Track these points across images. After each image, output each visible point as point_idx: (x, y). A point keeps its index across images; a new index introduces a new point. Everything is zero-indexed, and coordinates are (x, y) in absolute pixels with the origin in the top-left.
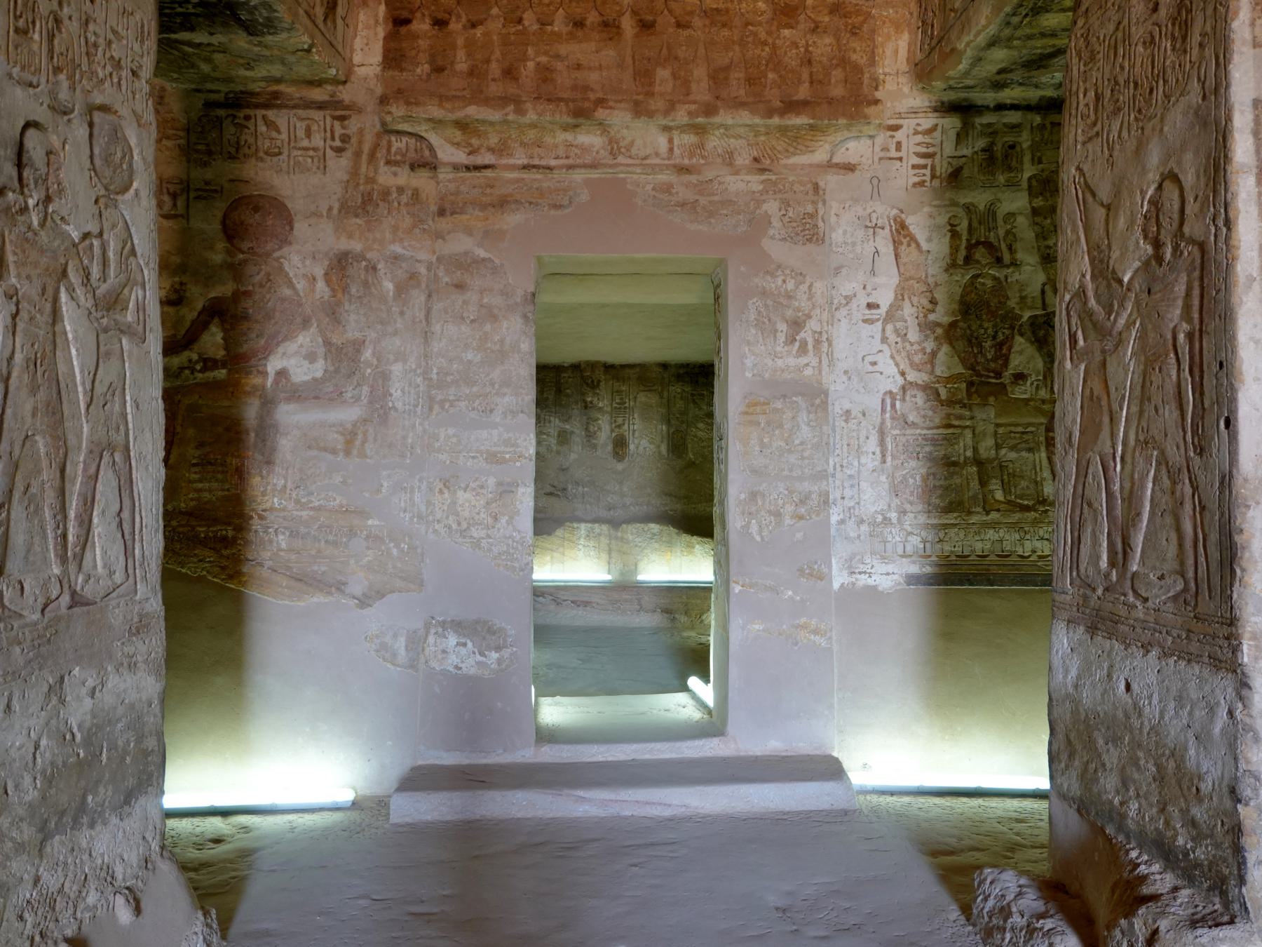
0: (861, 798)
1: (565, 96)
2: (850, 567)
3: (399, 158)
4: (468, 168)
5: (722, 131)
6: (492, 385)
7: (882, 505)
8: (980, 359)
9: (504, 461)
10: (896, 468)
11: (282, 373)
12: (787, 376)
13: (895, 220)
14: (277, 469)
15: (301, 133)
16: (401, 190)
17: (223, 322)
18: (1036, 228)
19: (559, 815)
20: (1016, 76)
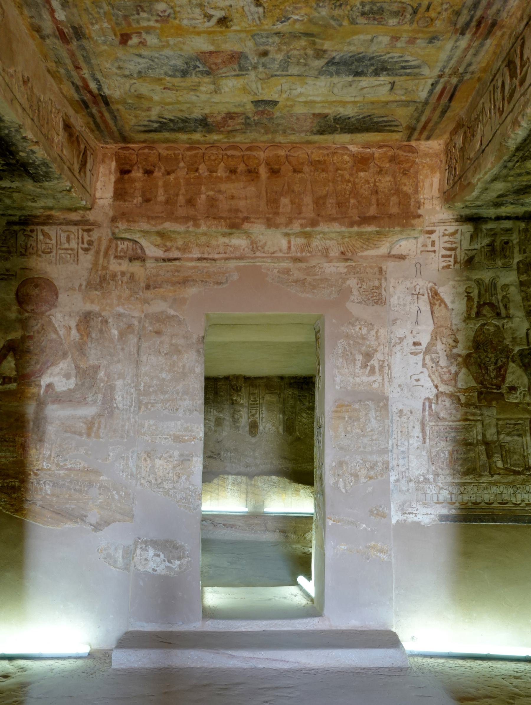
0: (411, 659)
1: (224, 216)
2: (402, 510)
3: (122, 254)
4: (164, 260)
5: (321, 235)
6: (178, 393)
7: (423, 470)
8: (486, 377)
9: (183, 441)
10: (432, 446)
11: (50, 386)
12: (362, 388)
13: (431, 290)
14: (46, 445)
15: (64, 240)
16: (123, 274)
17: (15, 354)
18: (523, 294)
19: (217, 666)
20: (509, 199)
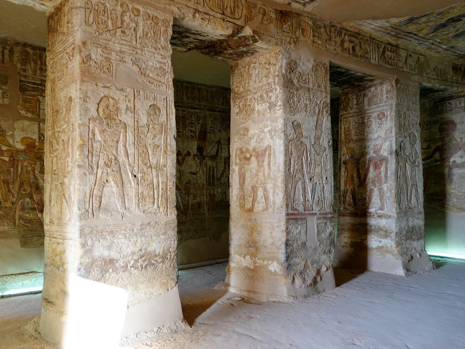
11: (454, 162)
14: (453, 184)
15: (458, 104)
